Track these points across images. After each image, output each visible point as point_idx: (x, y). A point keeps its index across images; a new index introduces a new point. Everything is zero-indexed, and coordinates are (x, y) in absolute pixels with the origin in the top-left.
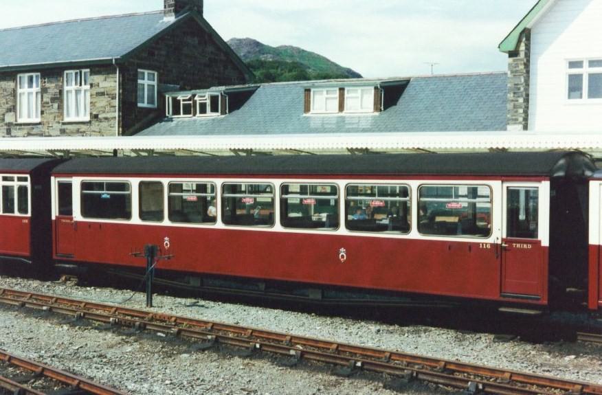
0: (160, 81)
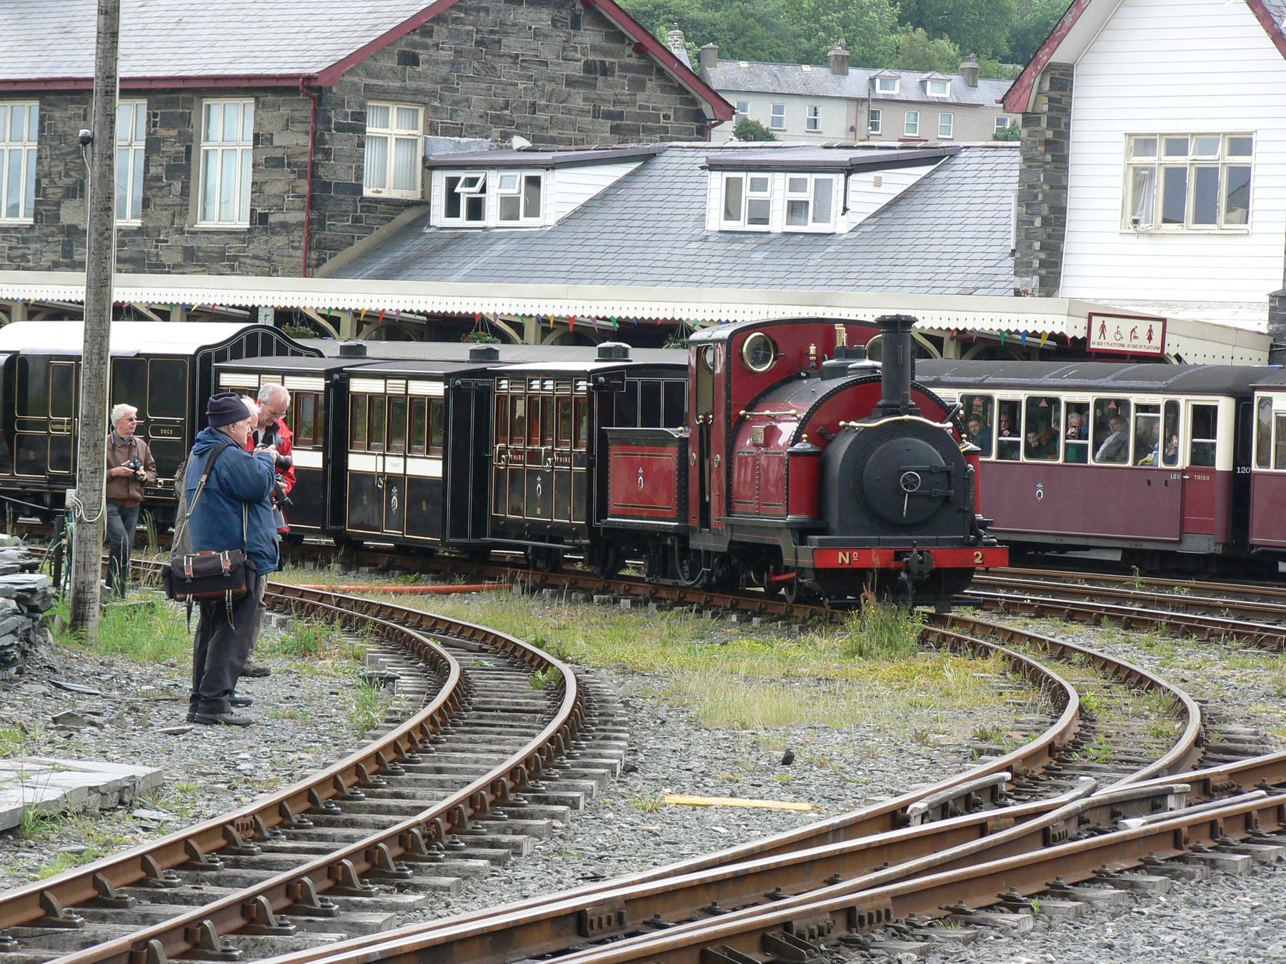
0: (431, 129)
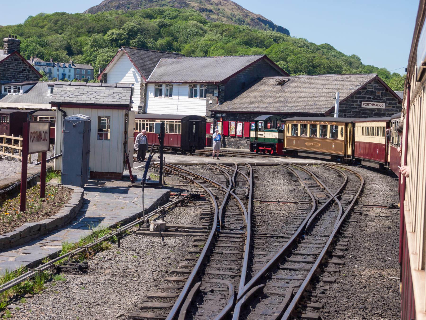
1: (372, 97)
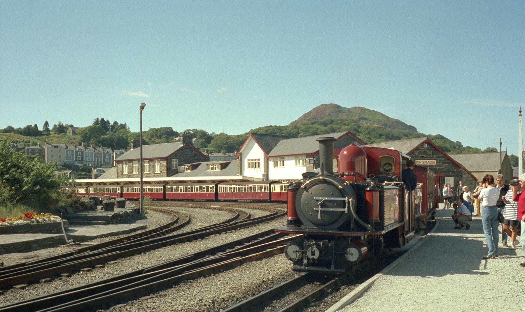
0: (178, 162)
1: (424, 156)
